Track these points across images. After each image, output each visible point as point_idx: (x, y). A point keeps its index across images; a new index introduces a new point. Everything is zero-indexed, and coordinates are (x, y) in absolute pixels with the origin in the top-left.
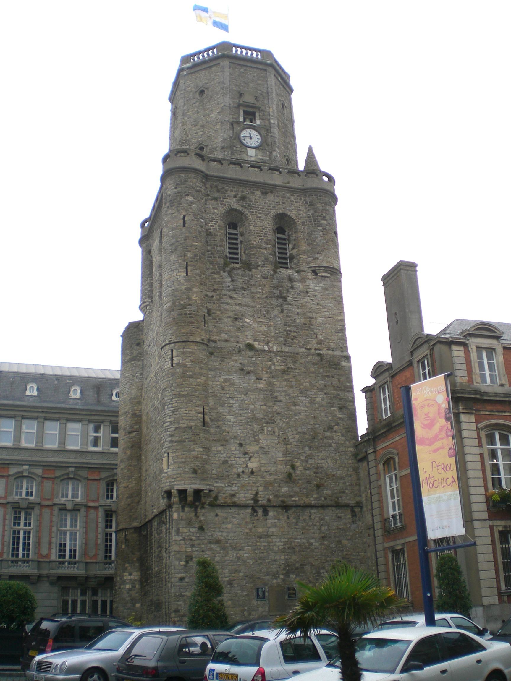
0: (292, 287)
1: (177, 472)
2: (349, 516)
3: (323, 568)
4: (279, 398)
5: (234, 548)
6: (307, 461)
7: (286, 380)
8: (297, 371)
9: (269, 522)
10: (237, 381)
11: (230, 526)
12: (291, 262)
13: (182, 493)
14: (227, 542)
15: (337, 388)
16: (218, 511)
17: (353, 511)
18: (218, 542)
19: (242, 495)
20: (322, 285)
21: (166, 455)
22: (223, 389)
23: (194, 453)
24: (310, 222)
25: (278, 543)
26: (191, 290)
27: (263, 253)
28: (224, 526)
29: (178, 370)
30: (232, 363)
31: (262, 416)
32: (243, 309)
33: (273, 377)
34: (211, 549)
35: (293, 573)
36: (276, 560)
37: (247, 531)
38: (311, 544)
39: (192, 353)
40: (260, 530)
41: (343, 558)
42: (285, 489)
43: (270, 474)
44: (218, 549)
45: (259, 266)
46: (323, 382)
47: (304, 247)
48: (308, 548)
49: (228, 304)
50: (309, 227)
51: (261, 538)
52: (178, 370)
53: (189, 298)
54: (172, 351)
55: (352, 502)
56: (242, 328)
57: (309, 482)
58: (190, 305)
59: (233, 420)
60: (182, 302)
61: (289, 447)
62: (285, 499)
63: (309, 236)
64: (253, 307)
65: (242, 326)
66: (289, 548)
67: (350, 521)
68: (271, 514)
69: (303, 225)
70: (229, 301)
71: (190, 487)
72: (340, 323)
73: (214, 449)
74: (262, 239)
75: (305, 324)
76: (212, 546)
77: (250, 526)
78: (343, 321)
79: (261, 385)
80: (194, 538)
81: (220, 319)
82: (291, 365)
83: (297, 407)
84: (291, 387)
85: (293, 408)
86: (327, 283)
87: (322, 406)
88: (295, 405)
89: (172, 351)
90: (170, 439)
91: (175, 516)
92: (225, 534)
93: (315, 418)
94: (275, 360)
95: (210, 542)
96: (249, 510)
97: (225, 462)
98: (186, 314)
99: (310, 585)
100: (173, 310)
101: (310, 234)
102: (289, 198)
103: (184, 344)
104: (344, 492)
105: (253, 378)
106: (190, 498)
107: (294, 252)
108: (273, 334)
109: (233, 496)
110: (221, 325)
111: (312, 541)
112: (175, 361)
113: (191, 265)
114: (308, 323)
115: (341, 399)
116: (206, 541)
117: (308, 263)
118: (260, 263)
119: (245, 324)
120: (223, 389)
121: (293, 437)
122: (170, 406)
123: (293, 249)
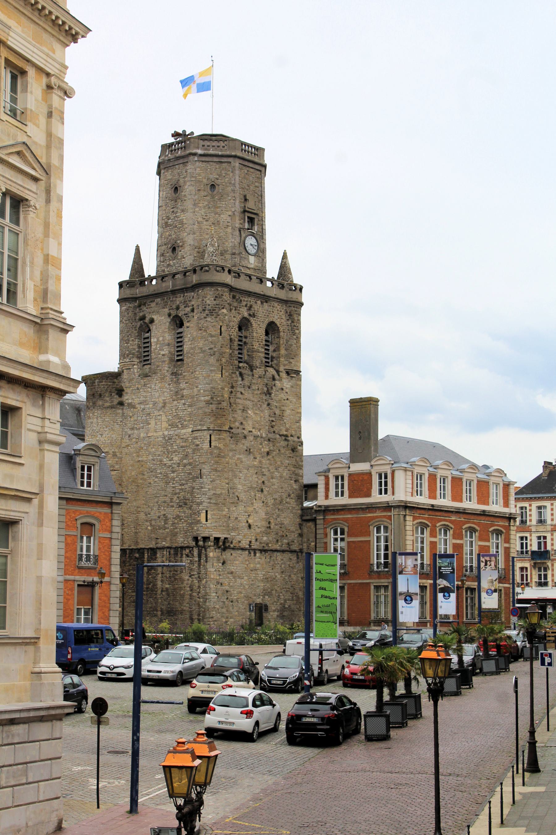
0: (274, 385)
1: (215, 525)
2: (296, 558)
3: (281, 593)
4: (264, 473)
5: (239, 577)
6: (276, 519)
7: (269, 459)
8: (275, 453)
9: (257, 560)
10: (244, 460)
11: (237, 562)
12: (272, 361)
13: (217, 539)
14: (236, 573)
15: (295, 466)
16: (232, 552)
17: (297, 555)
18: (232, 573)
19: (244, 542)
20: (290, 384)
21: (205, 511)
22: (236, 465)
23: (224, 513)
24: (289, 330)
25: (260, 575)
26: (224, 389)
27: (260, 357)
28: (235, 562)
29: (215, 451)
30: (241, 446)
31: (255, 486)
32: (248, 403)
33: (263, 457)
34: (228, 578)
35: (267, 595)
36: (259, 586)
37: (246, 566)
38: (276, 577)
39: (224, 439)
40: (252, 566)
41: (292, 586)
42: (265, 538)
43: (258, 528)
44: (232, 578)
45: (257, 367)
46: (287, 461)
47: (283, 352)
48: (274, 579)
49: (240, 398)
50: (287, 334)
51: (252, 571)
52: (215, 451)
53: (222, 396)
54: (210, 436)
55: (297, 549)
56: (246, 418)
57: (277, 534)
58: (223, 401)
59: (241, 488)
60: (218, 399)
61: (268, 508)
62: (265, 545)
63: (287, 343)
64: (253, 401)
65: (247, 417)
66: (266, 579)
67: (296, 561)
68: (258, 555)
69: (284, 332)
70: (240, 396)
71: (222, 536)
72: (299, 415)
73: (231, 509)
74: (260, 344)
75: (280, 415)
76: (229, 575)
77: (247, 563)
78: (300, 413)
79: (256, 463)
80: (220, 570)
81: (235, 411)
82: (272, 448)
83: (274, 480)
84: (271, 465)
85: (271, 480)
86: (294, 381)
87: (286, 479)
88: (272, 478)
89: (210, 436)
90: (209, 501)
91: (211, 554)
92: (235, 568)
93: (282, 488)
94: (264, 444)
95: (228, 573)
96: (247, 552)
97: (236, 518)
98: (221, 409)
99: (275, 603)
100: (211, 404)
101: (287, 341)
102: (276, 308)
103: (219, 432)
104: (294, 542)
105: (252, 457)
106: (221, 543)
107: (274, 355)
108: (262, 423)
109: (240, 542)
110: (236, 416)
111: (277, 574)
112: (213, 444)
113: (225, 369)
114: (281, 414)
115: (296, 475)
116: (226, 572)
117: (284, 365)
118: (258, 365)
119: (248, 415)
120: (236, 465)
121: (270, 502)
122: (209, 477)
123: (274, 351)
